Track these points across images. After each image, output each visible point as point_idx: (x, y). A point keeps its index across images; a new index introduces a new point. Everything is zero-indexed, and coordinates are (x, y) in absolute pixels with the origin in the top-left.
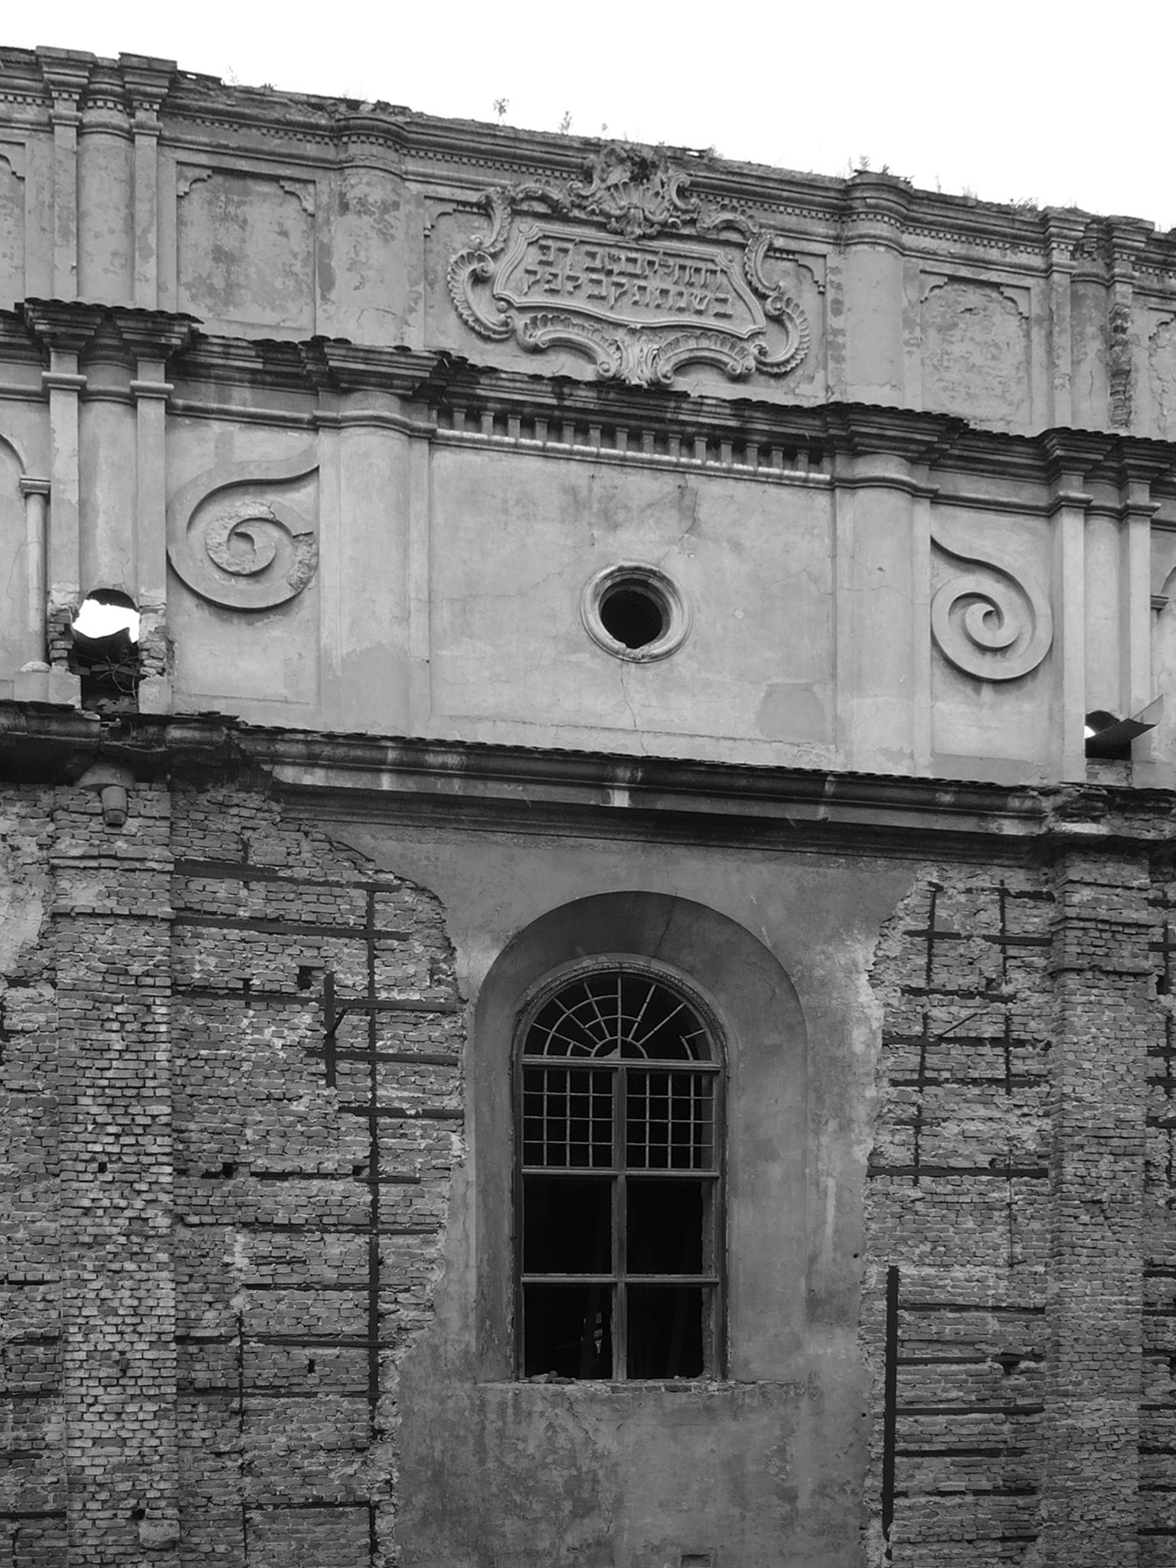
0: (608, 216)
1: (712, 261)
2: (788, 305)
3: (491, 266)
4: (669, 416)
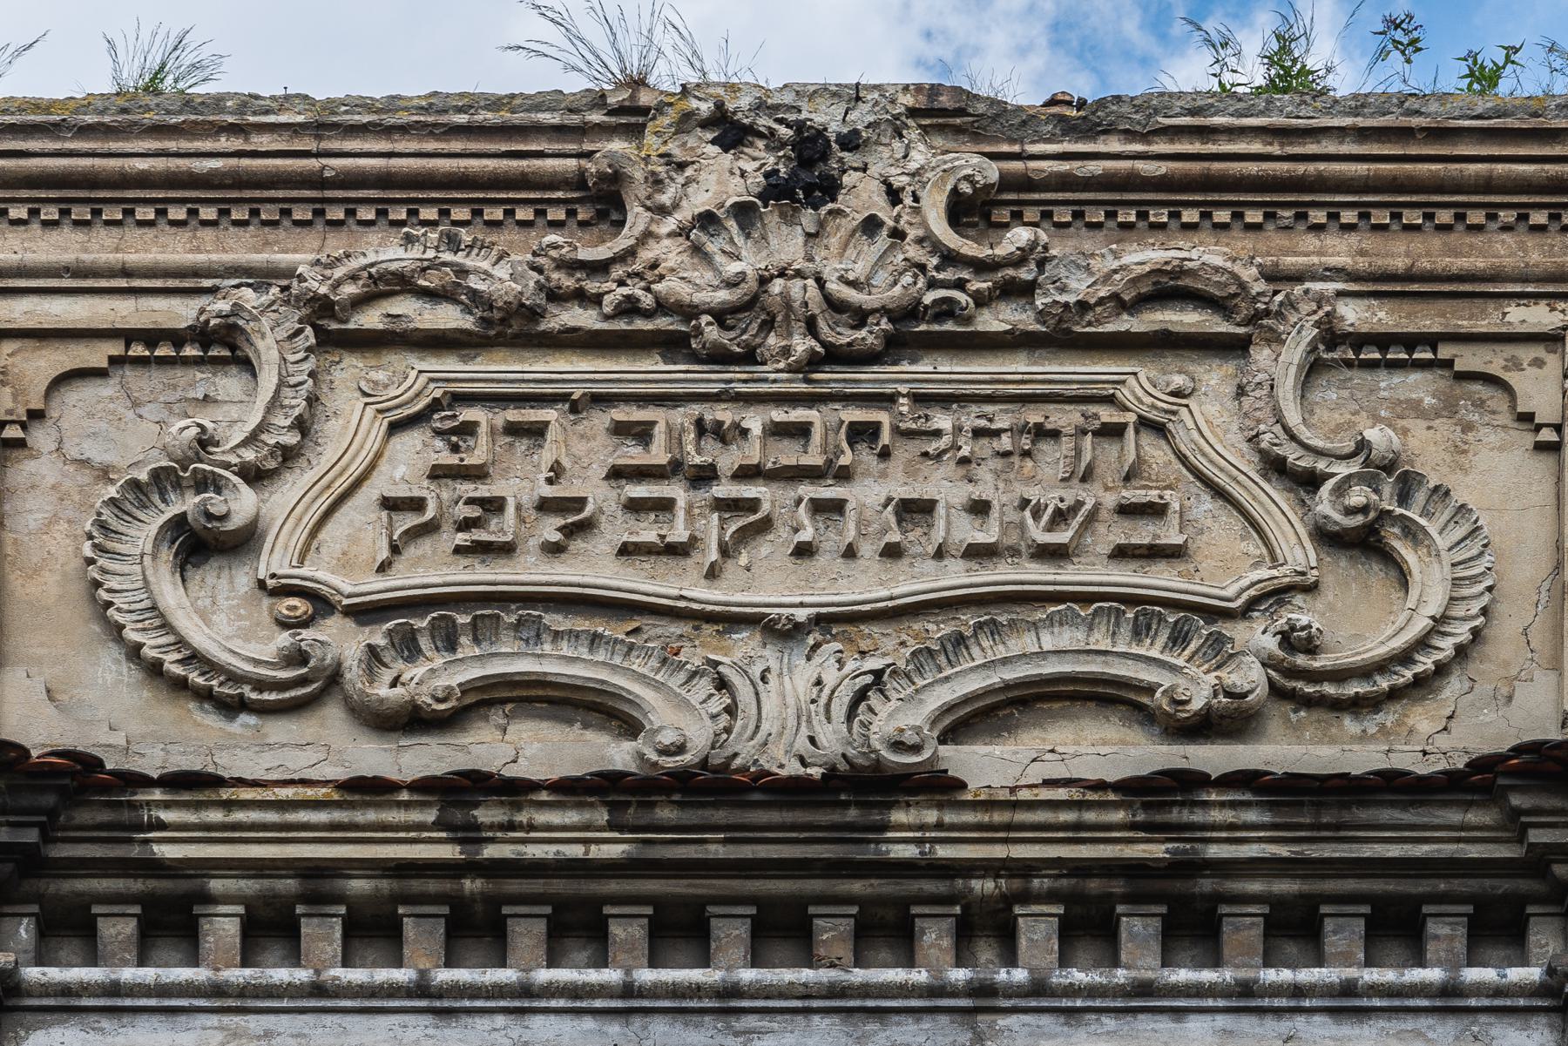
0: (690, 312)
1: (1110, 400)
2: (1404, 498)
3: (242, 503)
4: (909, 852)
